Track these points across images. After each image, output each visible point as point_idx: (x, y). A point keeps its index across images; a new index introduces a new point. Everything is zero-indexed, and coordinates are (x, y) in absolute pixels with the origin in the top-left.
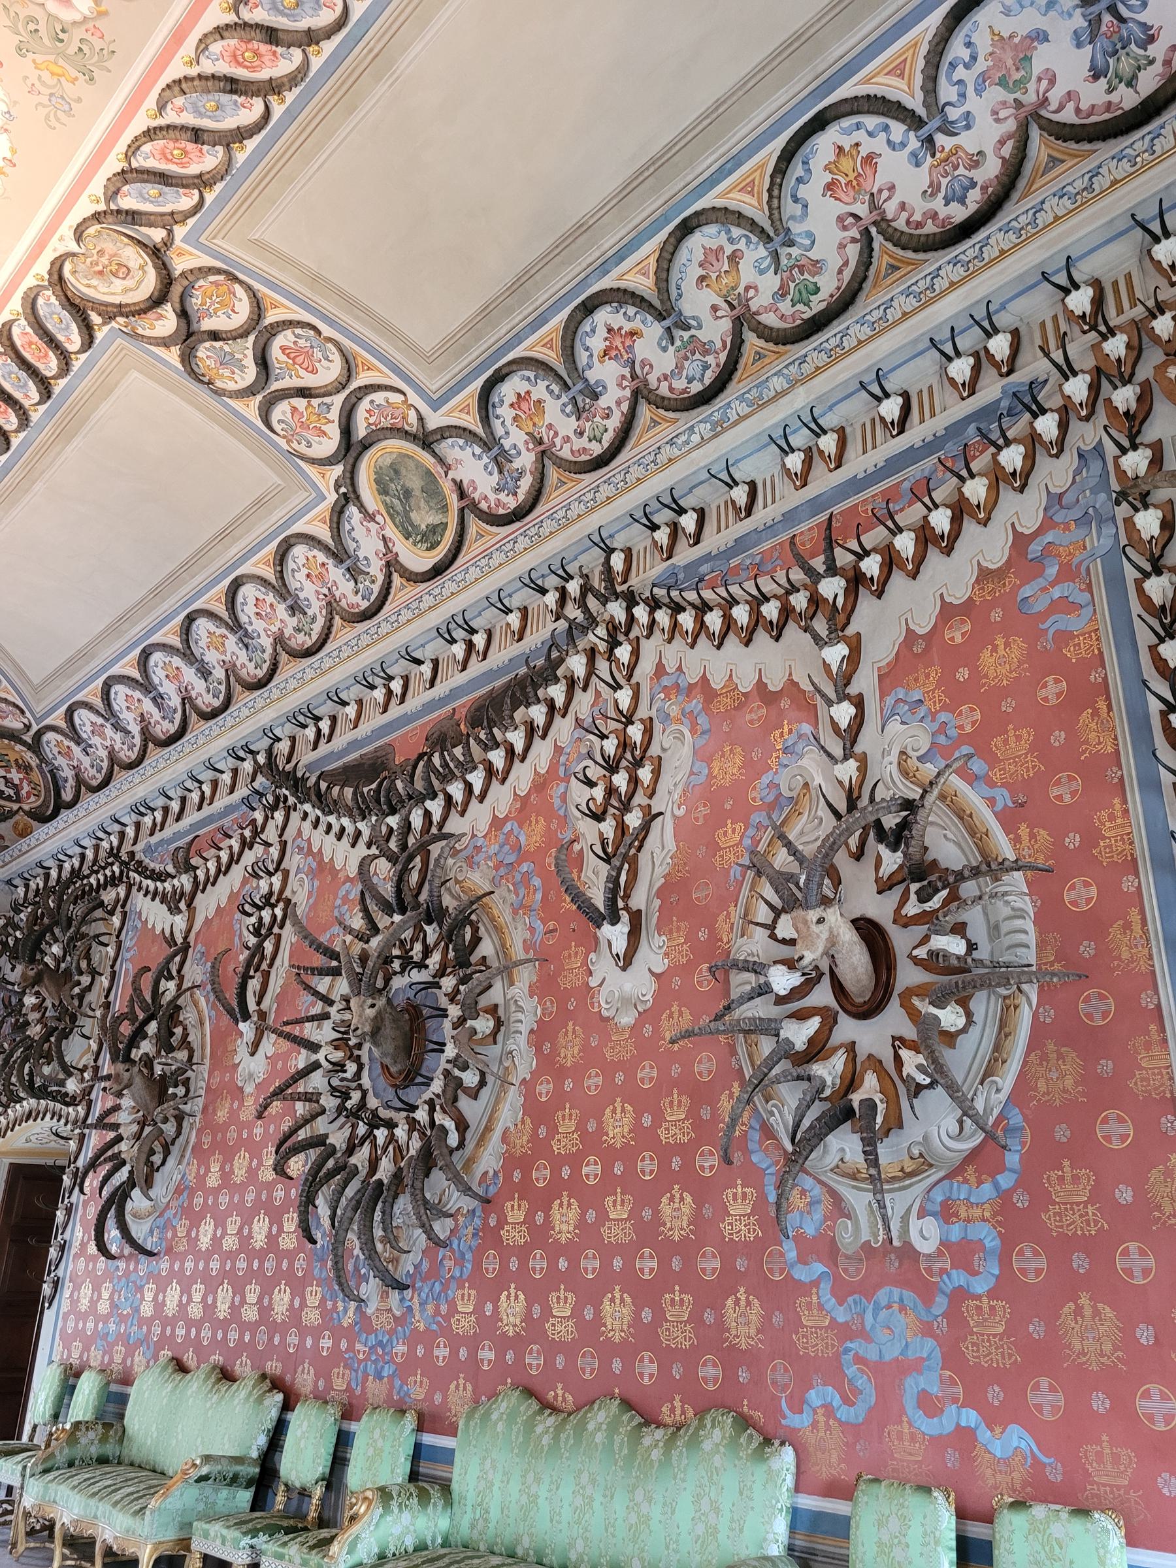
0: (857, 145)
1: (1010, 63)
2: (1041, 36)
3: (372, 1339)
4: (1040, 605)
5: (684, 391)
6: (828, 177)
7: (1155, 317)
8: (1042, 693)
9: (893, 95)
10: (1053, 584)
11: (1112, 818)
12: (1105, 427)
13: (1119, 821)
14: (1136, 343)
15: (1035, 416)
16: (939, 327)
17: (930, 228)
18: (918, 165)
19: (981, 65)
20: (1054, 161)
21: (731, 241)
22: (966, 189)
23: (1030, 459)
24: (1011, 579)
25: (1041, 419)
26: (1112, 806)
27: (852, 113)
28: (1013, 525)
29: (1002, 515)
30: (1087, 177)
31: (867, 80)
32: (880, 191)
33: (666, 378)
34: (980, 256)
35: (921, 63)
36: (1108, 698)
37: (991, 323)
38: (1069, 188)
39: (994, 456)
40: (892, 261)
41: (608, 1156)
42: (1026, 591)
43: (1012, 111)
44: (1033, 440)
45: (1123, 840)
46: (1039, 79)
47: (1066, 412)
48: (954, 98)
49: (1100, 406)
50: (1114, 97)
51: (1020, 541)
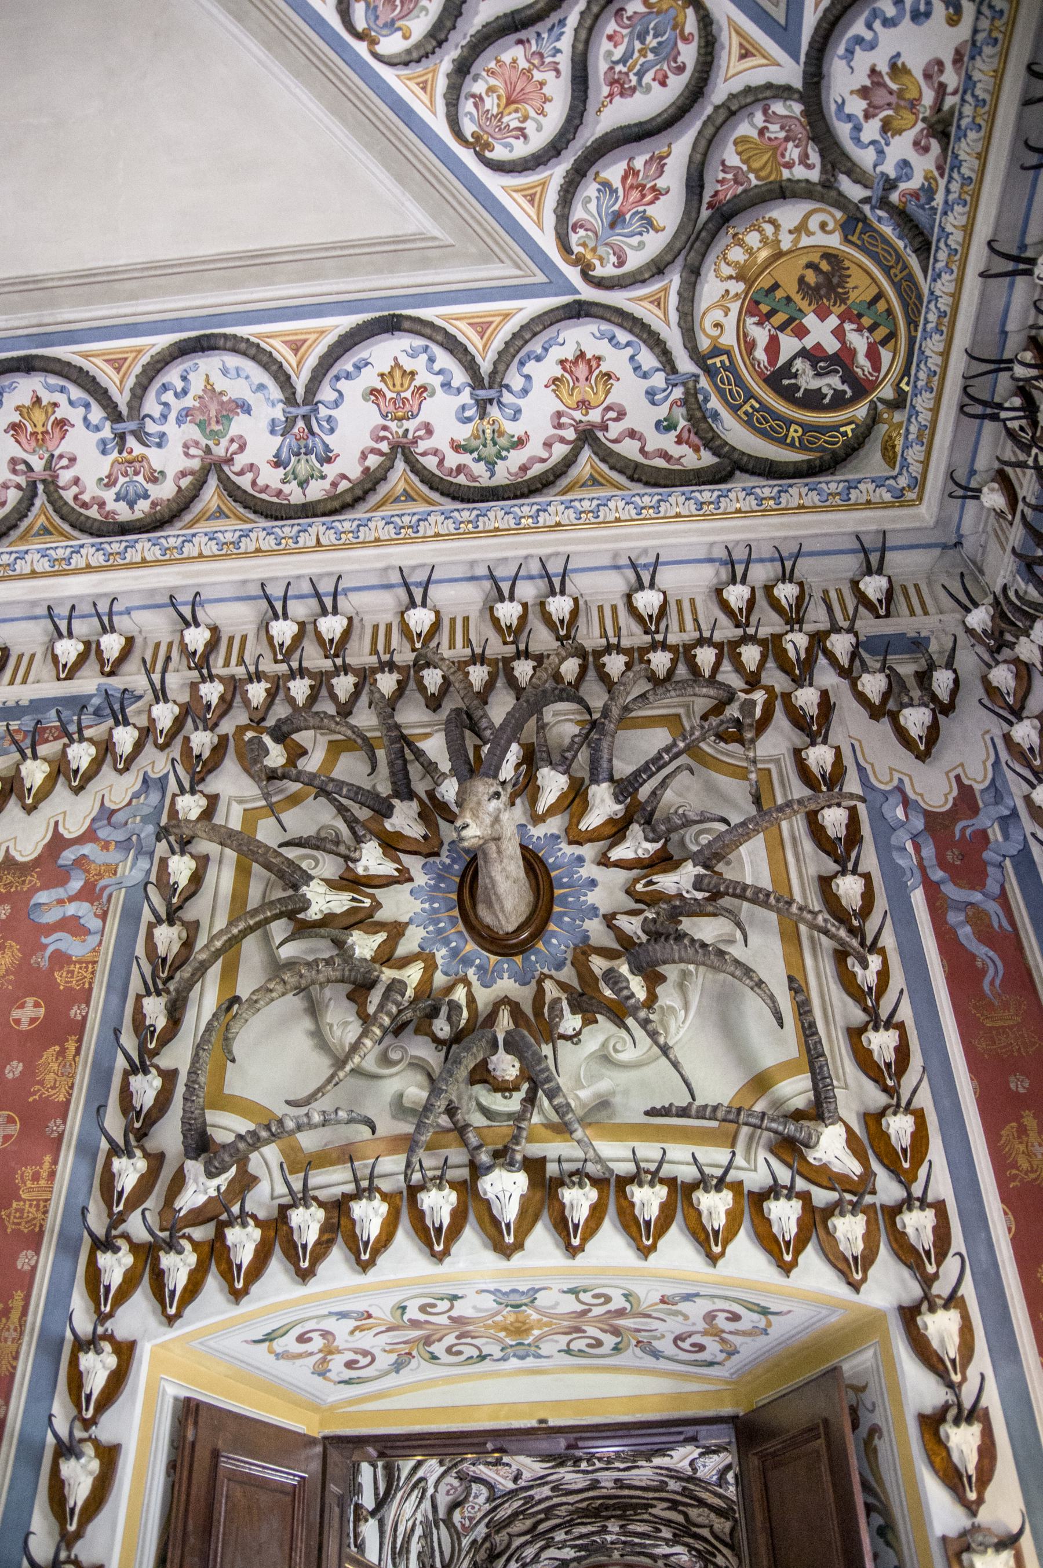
0: (55, 405)
1: (213, 413)
2: (246, 408)
4: (50, 917)
6: (16, 418)
7: (251, 681)
8: (16, 1014)
9: (104, 381)
10: (71, 899)
11: (36, 1177)
12: (173, 760)
13: (42, 1183)
14: (228, 697)
15: (117, 723)
16: (61, 601)
17: (93, 513)
18: (104, 452)
19: (189, 401)
20: (220, 514)
22: (139, 497)
23: (97, 764)
24: (33, 879)
25: (121, 728)
26: (41, 1165)
27: (66, 377)
28: (56, 823)
29: (48, 810)
30: (238, 534)
31: (86, 356)
32: (61, 457)
34: (122, 554)
35: (138, 369)
36: (80, 1041)
37: (111, 621)
38: (219, 535)
39: (65, 746)
40: (46, 523)
42: (43, 897)
43: (201, 453)
44: (106, 747)
45: (38, 1206)
46: (232, 441)
47: (147, 732)
48: (157, 415)
49: (179, 741)
50: (286, 489)
51: (57, 843)
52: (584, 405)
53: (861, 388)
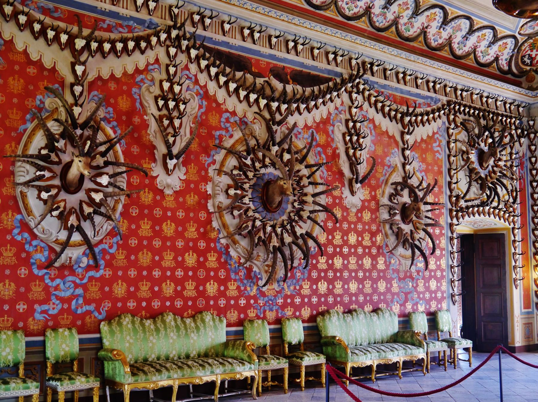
3: (266, 299)
5: (375, 22)
21: (411, 5)
33: (374, 14)
41: (350, 247)
52: (500, 51)
53: (531, 64)
